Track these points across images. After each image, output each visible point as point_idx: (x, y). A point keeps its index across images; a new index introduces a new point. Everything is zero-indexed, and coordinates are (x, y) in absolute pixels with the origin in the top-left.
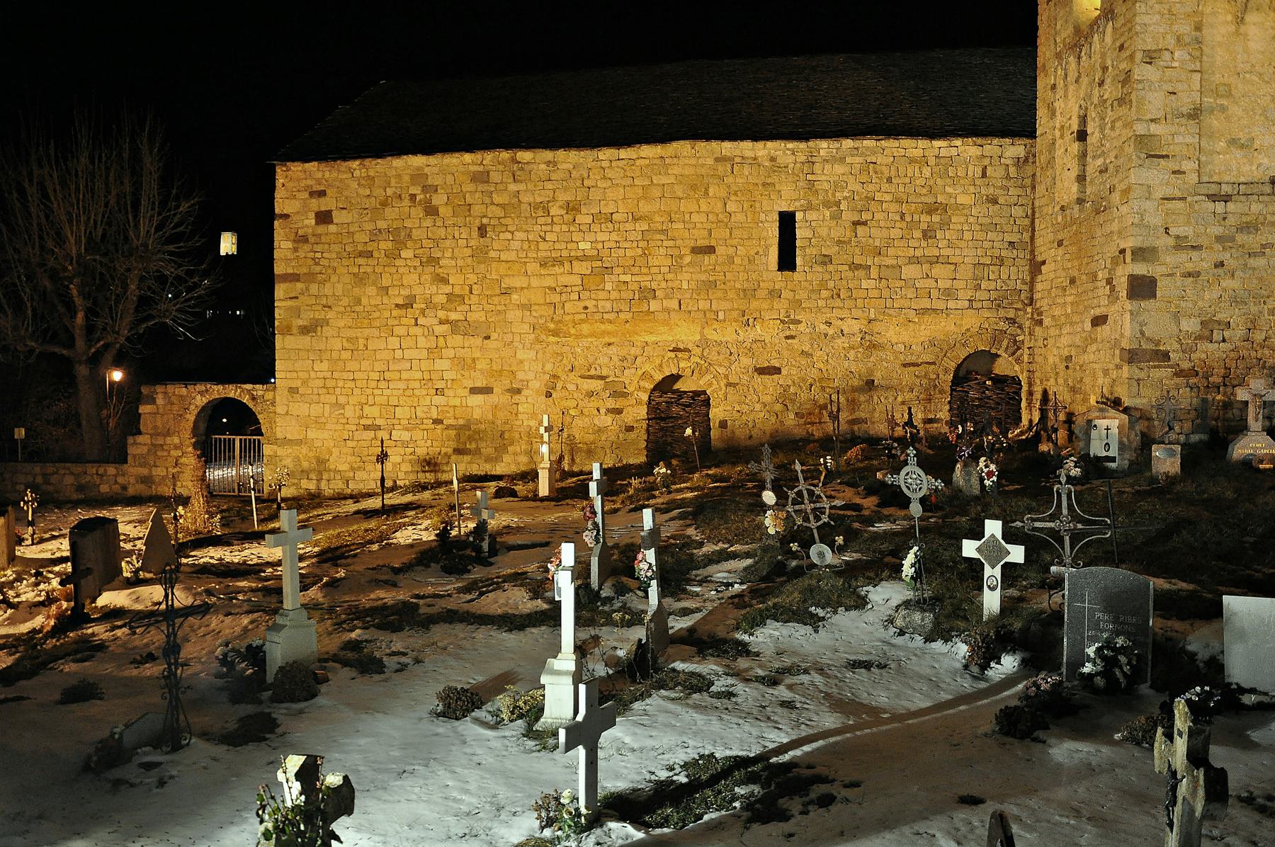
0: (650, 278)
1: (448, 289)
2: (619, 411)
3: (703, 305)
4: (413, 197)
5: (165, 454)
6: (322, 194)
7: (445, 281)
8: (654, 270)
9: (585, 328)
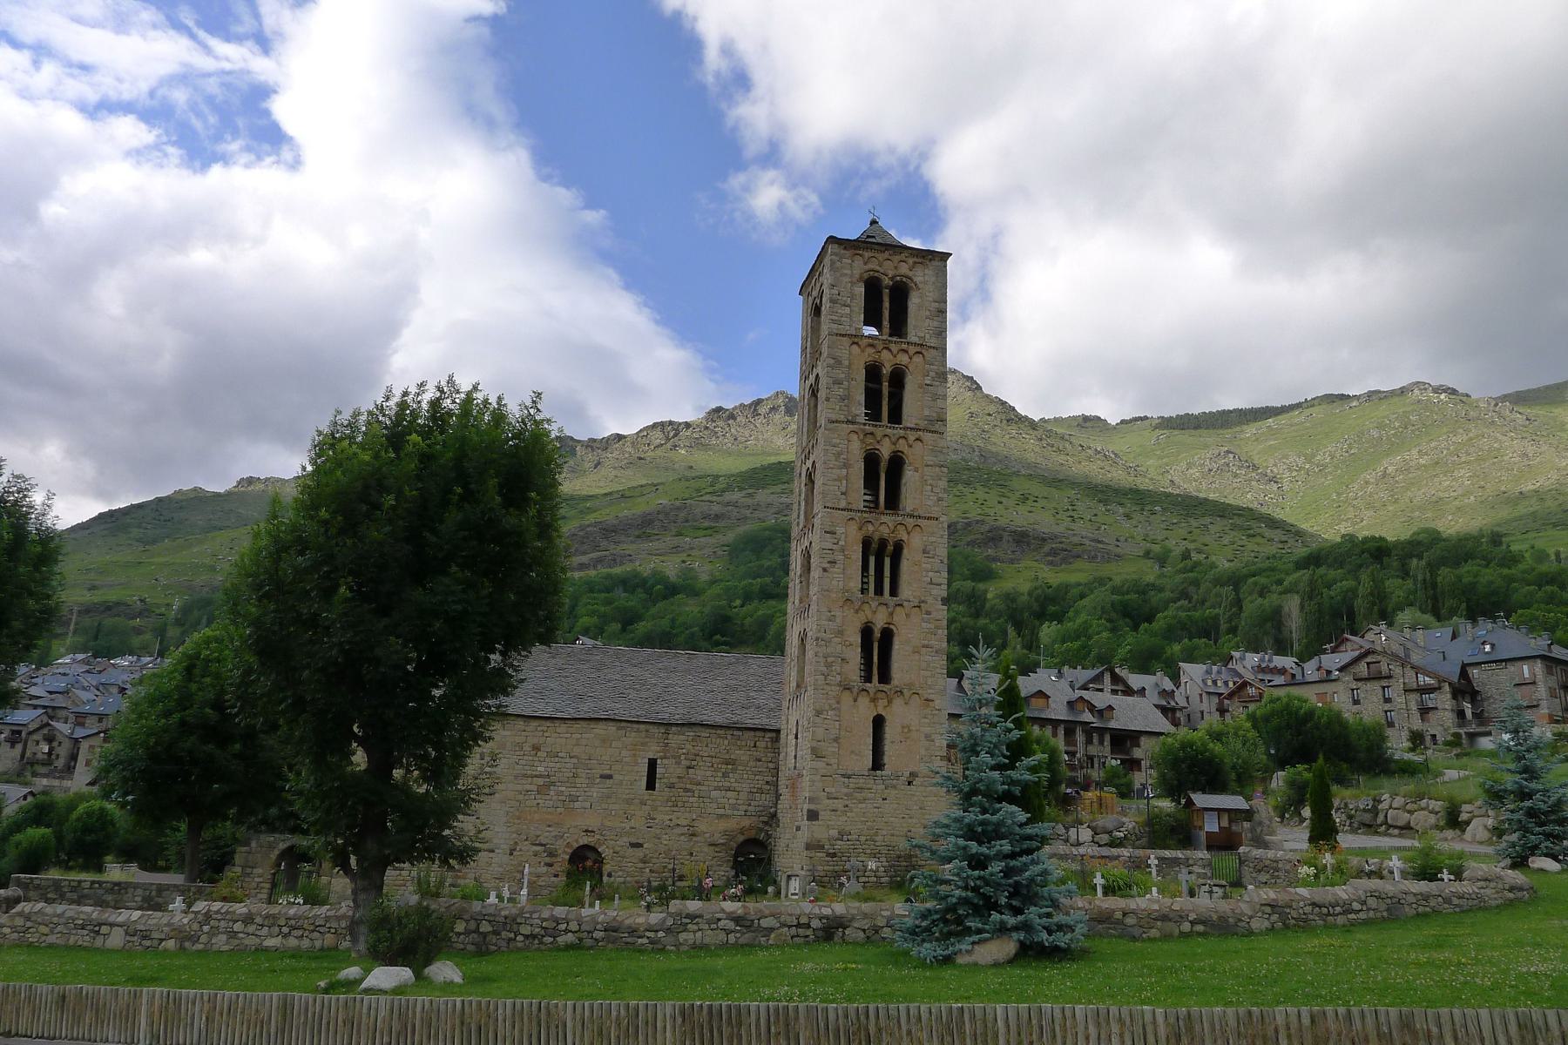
0: (576, 789)
2: (550, 865)
3: (603, 806)
5: (250, 880)
8: (578, 785)
9: (537, 816)
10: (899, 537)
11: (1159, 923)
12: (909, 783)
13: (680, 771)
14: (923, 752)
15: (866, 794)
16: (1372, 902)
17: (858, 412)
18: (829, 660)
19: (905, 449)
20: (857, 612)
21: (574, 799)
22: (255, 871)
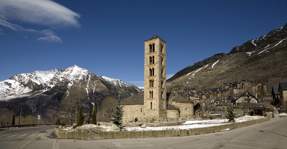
16: (134, 125)
21: (135, 113)
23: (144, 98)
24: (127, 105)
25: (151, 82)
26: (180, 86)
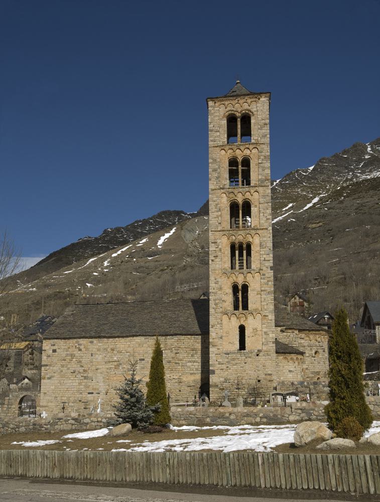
1: (83, 368)
3: (142, 372)
4: (76, 346)
6: (54, 345)
7: (82, 367)
9: (115, 378)
10: (248, 240)
11: (246, 418)
12: (257, 355)
13: (173, 355)
14: (264, 340)
15: (237, 361)
17: (226, 183)
18: (217, 301)
19: (250, 197)
20: (228, 278)
22: (12, 406)
23: (212, 311)
24: (91, 337)
25: (237, 252)
26: (69, 297)
